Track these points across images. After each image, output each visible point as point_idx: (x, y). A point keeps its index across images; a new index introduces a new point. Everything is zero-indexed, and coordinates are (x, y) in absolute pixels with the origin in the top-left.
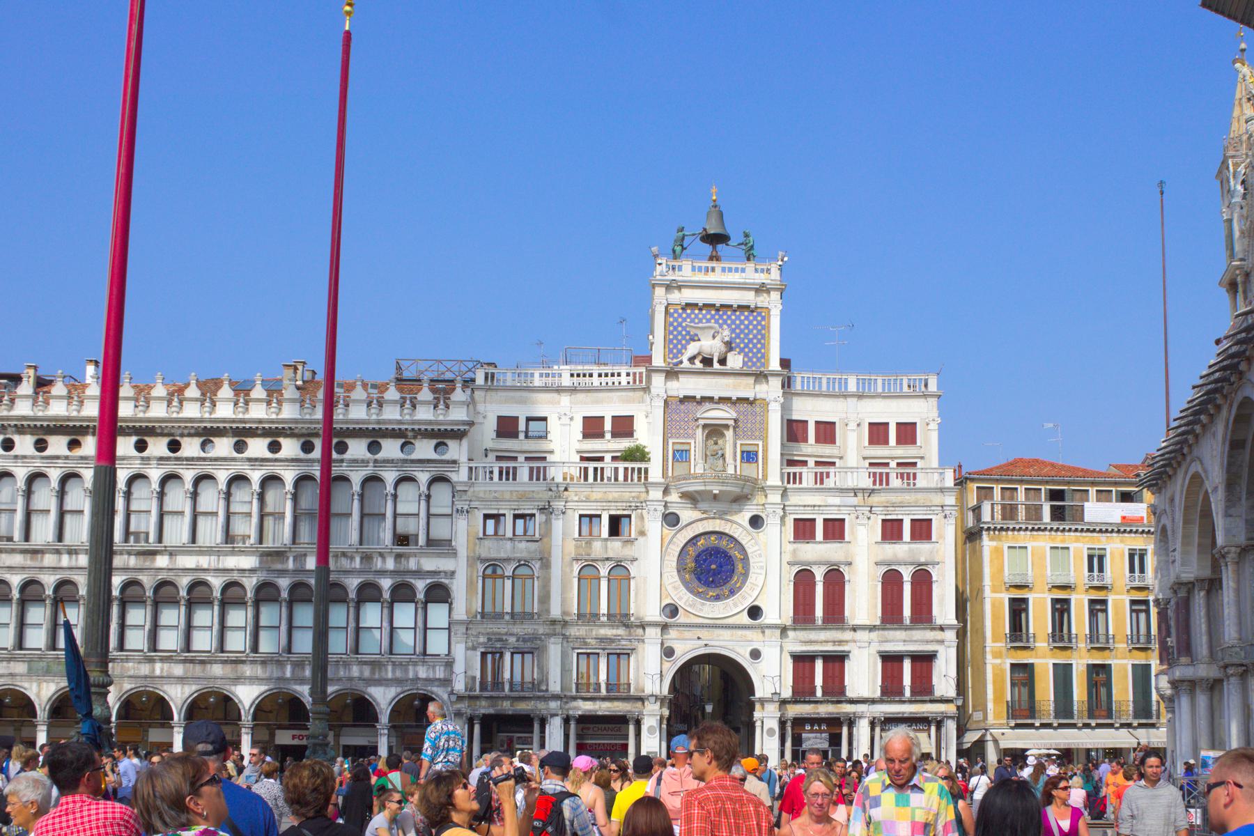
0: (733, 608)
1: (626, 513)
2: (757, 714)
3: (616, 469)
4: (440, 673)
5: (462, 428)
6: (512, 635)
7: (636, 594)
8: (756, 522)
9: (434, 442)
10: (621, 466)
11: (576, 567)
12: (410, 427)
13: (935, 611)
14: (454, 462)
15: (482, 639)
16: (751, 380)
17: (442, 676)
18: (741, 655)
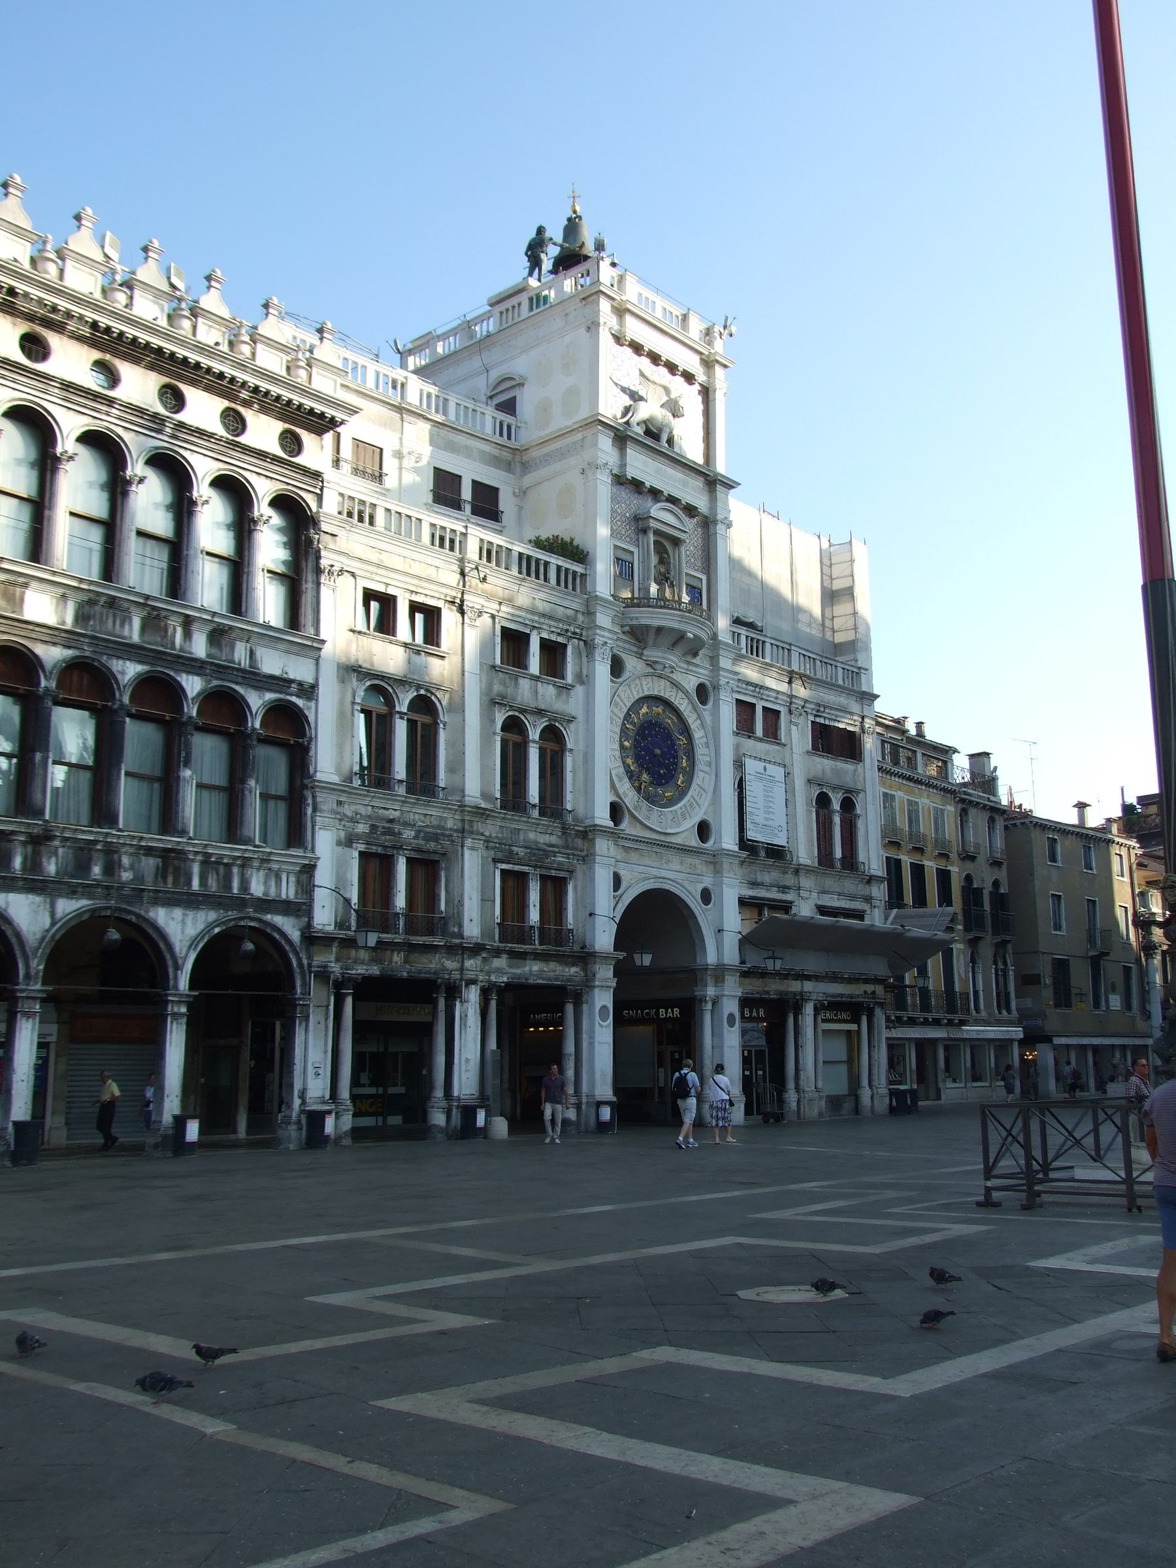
0: (677, 821)
1: (560, 640)
2: (711, 991)
3: (547, 564)
4: (288, 890)
5: (339, 416)
6: (406, 824)
7: (574, 780)
8: (702, 693)
9: (279, 426)
10: (555, 560)
11: (500, 717)
12: (252, 381)
13: (862, 857)
14: (317, 475)
15: (362, 828)
16: (699, 483)
17: (292, 896)
18: (691, 896)
